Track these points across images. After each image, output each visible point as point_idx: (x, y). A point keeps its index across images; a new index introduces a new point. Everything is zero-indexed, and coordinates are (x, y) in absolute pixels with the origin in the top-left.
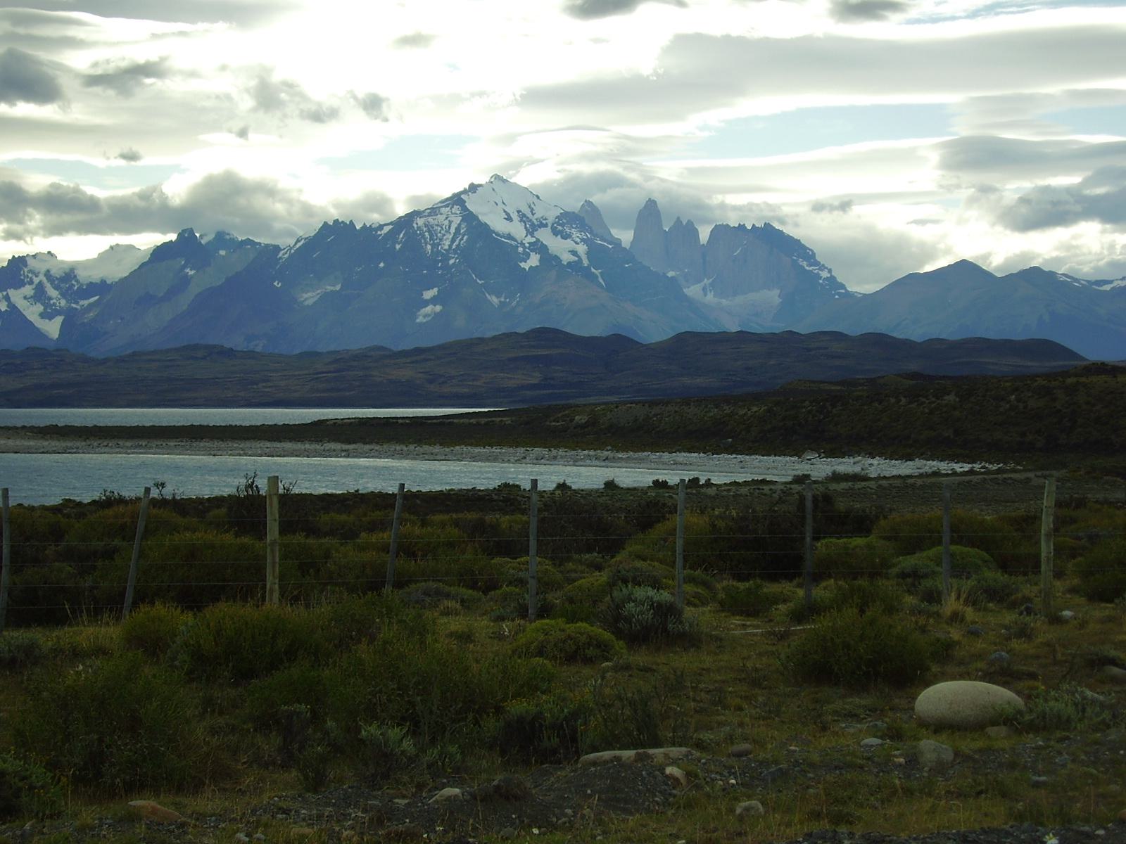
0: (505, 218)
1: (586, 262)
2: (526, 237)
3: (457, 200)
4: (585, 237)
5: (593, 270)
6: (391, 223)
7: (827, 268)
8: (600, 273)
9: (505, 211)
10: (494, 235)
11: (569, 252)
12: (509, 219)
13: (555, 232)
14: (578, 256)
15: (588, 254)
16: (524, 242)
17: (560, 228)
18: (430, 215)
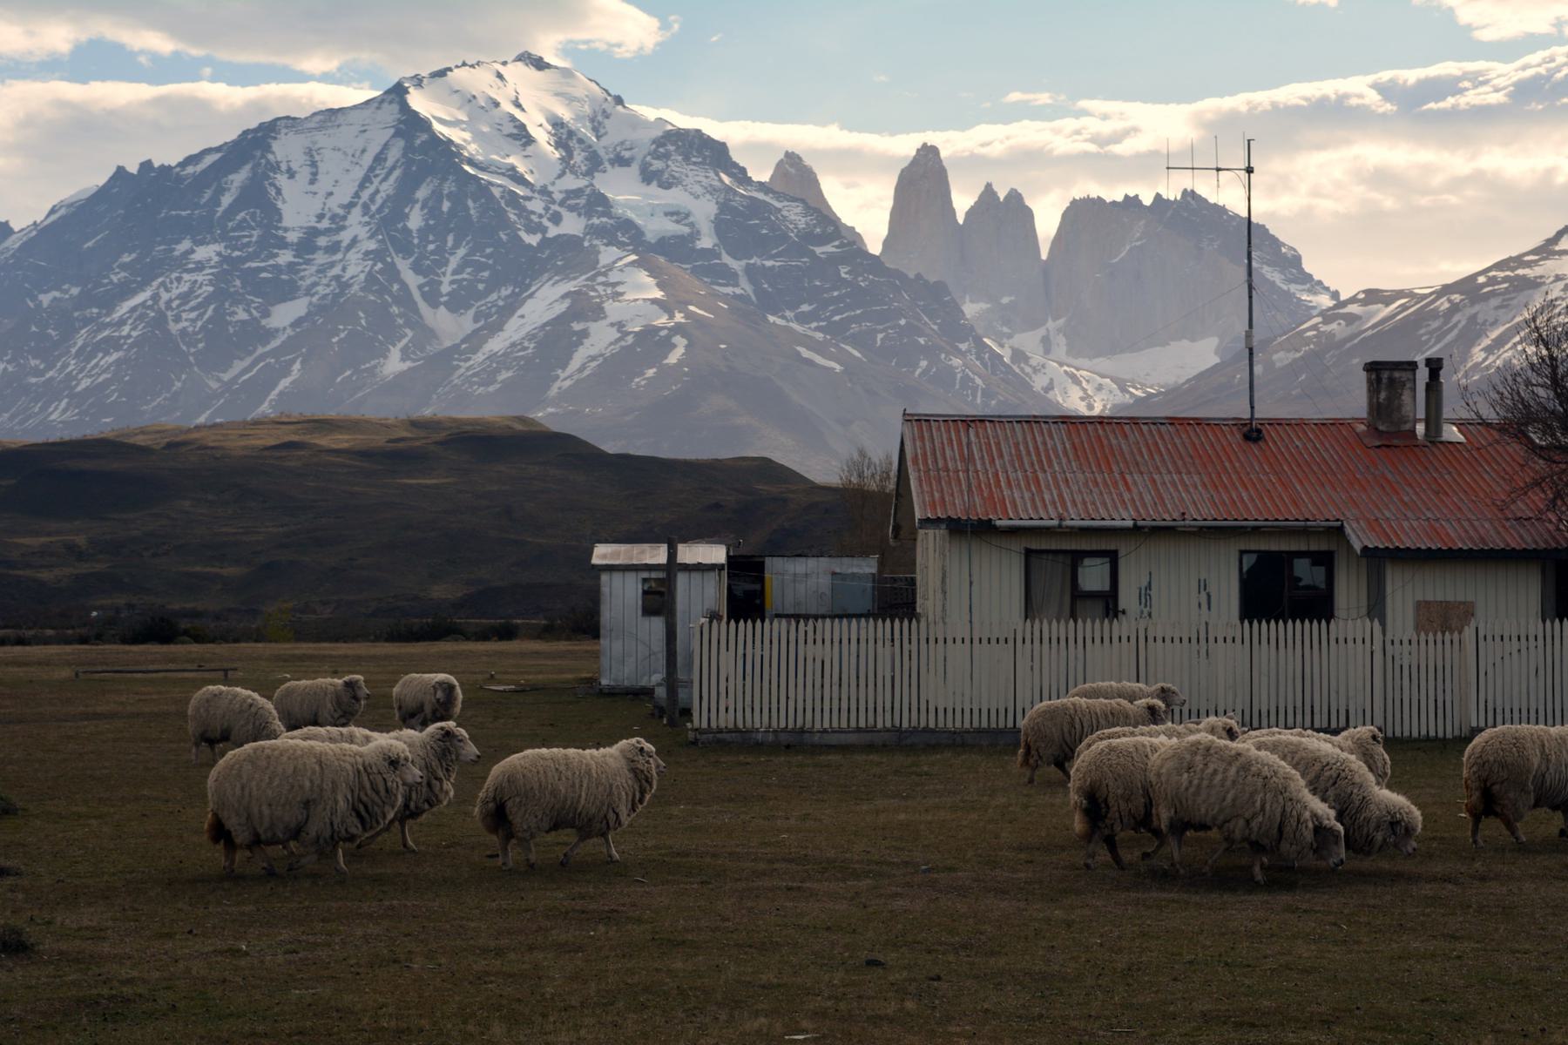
0: (510, 135)
1: (706, 242)
2: (560, 176)
3: (398, 92)
4: (716, 183)
5: (727, 259)
6: (218, 149)
7: (1327, 289)
8: (750, 271)
9: (513, 119)
10: (467, 168)
11: (666, 214)
12: (522, 136)
13: (648, 176)
14: (692, 225)
15: (720, 226)
16: (550, 188)
17: (657, 165)
18: (320, 128)
